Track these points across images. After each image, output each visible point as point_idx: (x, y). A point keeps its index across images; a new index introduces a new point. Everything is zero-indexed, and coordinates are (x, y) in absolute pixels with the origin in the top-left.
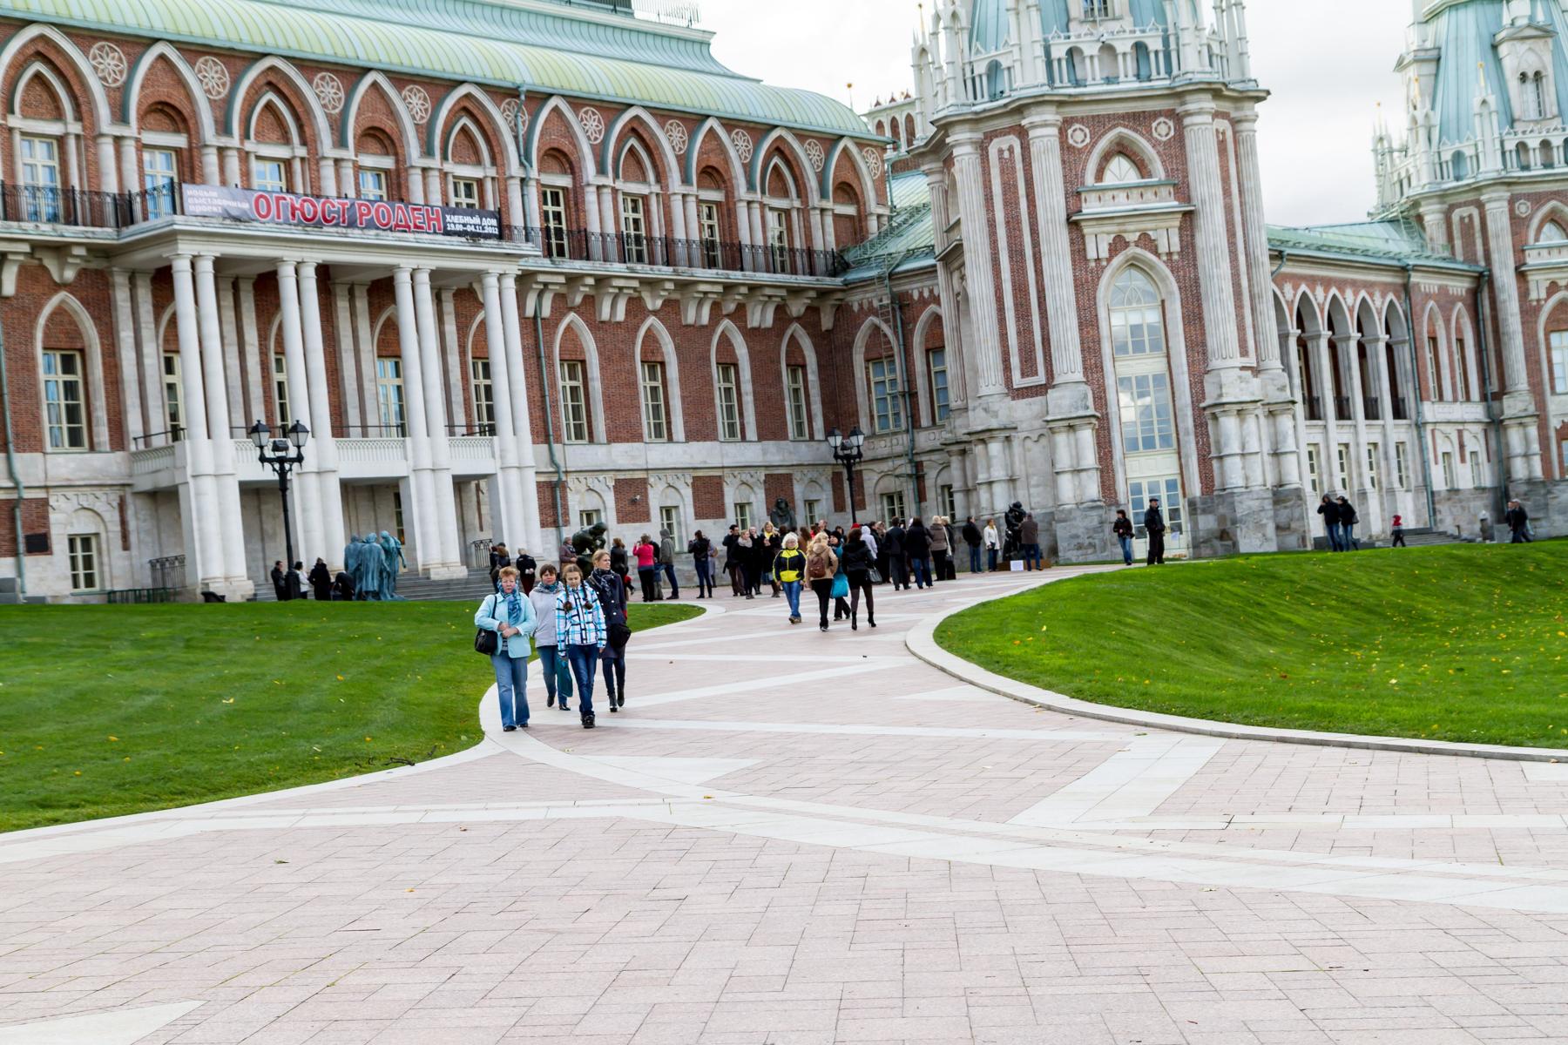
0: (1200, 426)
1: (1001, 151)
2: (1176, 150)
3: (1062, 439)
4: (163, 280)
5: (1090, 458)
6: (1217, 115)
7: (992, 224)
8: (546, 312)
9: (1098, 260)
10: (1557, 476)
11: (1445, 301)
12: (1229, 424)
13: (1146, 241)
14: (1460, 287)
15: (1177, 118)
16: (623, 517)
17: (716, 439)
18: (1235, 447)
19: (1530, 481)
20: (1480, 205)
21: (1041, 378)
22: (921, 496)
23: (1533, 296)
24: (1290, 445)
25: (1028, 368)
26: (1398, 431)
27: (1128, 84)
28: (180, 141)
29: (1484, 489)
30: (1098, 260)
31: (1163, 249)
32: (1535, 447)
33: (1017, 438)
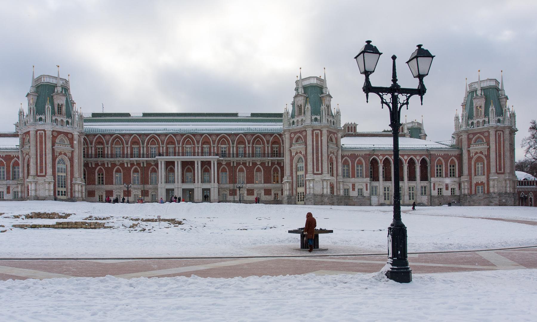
2: (305, 137)
4: (157, 165)
5: (288, 188)
8: (235, 165)
10: (473, 192)
12: (307, 183)
13: (301, 153)
15: (306, 131)
16: (248, 194)
17: (271, 183)
18: (307, 187)
19: (464, 195)
24: (325, 186)
26: (425, 183)
27: (300, 126)
28: (174, 146)
29: (456, 196)
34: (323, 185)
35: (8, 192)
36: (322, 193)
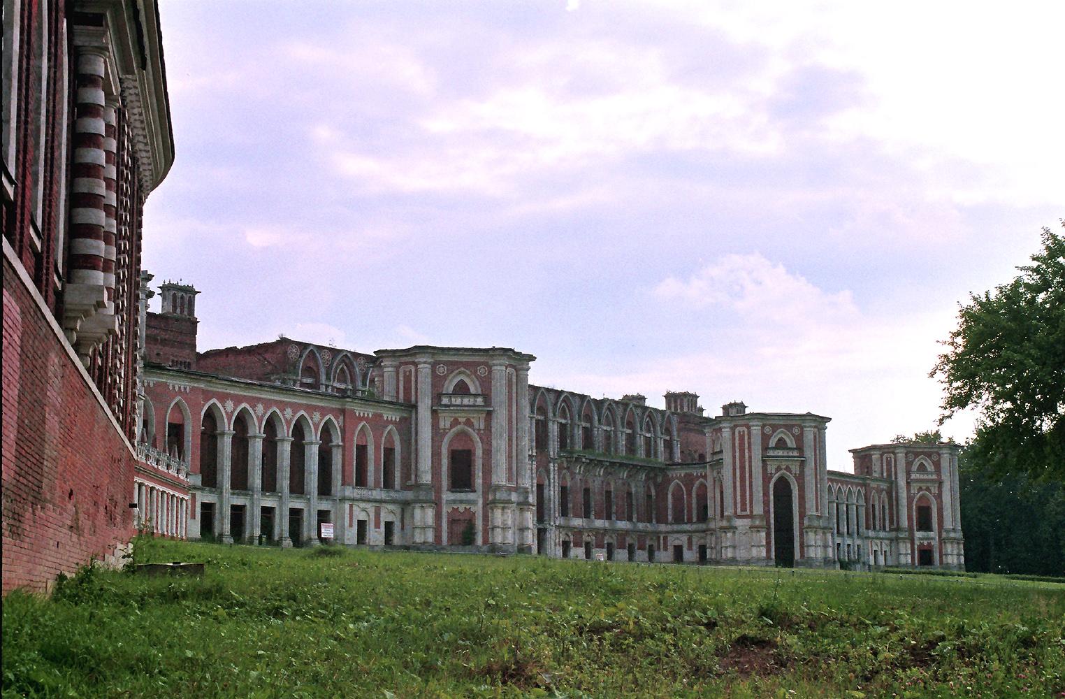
0: (801, 535)
1: (739, 432)
3: (754, 534)
6: (815, 427)
7: (734, 457)
9: (771, 474)
11: (880, 491)
14: (884, 486)
15: (802, 428)
20: (894, 453)
21: (748, 512)
22: (690, 548)
23: (913, 492)
25: (743, 509)
30: (771, 474)
31: (794, 472)
32: (910, 552)
33: (737, 532)
34: (825, 540)
35: (377, 526)
36: (823, 555)
